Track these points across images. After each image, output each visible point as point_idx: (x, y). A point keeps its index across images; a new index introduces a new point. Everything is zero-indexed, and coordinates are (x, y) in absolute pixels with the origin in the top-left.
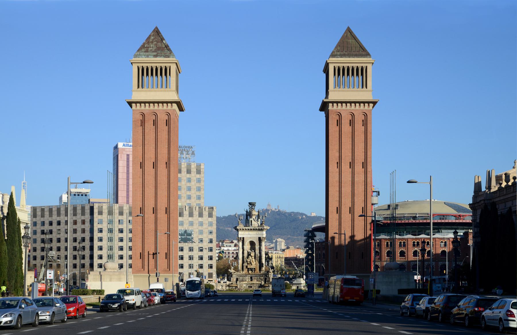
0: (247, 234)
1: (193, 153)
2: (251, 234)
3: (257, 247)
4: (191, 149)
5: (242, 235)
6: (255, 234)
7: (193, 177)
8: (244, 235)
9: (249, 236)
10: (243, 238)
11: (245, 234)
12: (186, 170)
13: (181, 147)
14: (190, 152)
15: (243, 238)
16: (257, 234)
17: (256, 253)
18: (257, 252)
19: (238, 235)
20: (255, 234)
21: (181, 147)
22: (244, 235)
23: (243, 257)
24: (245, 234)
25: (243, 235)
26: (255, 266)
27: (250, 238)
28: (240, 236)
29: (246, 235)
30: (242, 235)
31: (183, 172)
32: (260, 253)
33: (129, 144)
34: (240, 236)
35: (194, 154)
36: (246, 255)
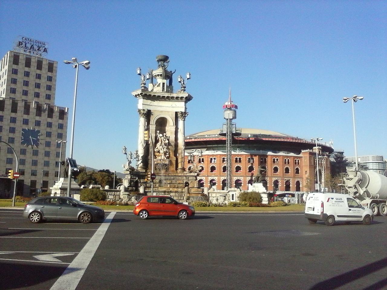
1: (45, 50)
4: (44, 45)
6: (169, 107)
13: (32, 41)
14: (42, 49)
16: (172, 107)
21: (32, 41)
25: (149, 105)
31: (32, 66)
35: (46, 51)
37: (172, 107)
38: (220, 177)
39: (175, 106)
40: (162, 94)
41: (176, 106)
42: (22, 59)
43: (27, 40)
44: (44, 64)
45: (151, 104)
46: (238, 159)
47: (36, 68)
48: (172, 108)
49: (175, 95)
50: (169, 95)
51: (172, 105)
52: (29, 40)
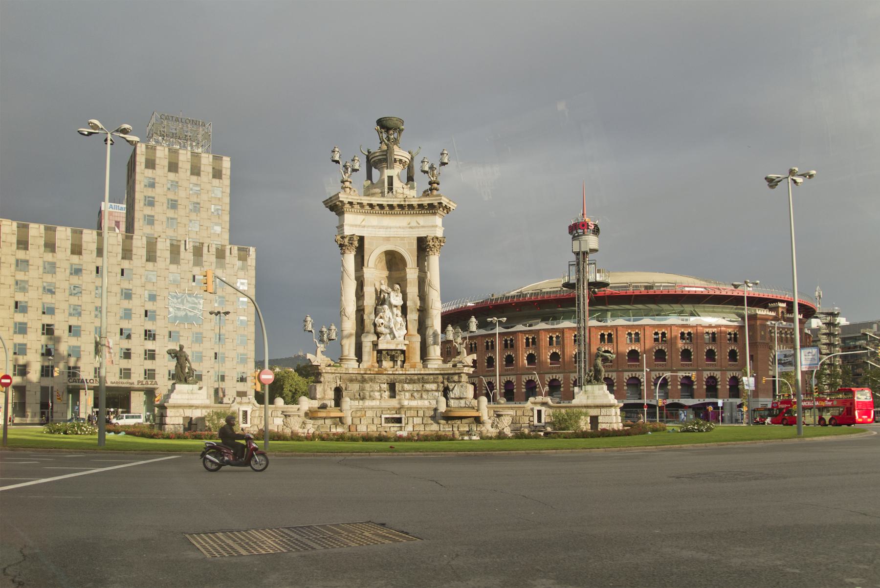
0: (373, 227)
2: (390, 228)
3: (412, 273)
5: (356, 226)
6: (403, 228)
7: (204, 182)
8: (364, 227)
9: (382, 233)
10: (361, 239)
11: (369, 227)
12: (189, 167)
15: (361, 239)
16: (411, 228)
17: (409, 296)
18: (413, 290)
19: (341, 227)
20: (403, 228)
21: (180, 120)
22: (364, 227)
23: (360, 311)
24: (369, 227)
25: (359, 226)
26: (407, 342)
27: (388, 239)
28: (348, 231)
29: (370, 229)
30: (356, 226)
31: (182, 170)
32: (423, 296)
33: (119, 206)
34: (348, 231)
36: (369, 301)
37: (411, 228)
38: (568, 374)
39: (414, 224)
40: (388, 201)
41: (419, 224)
42: (162, 156)
43: (171, 118)
44: (182, 161)
45: (363, 223)
46: (606, 337)
47: (189, 172)
48: (411, 230)
49: (415, 201)
50: (400, 201)
51: (409, 224)
52: (174, 119)
